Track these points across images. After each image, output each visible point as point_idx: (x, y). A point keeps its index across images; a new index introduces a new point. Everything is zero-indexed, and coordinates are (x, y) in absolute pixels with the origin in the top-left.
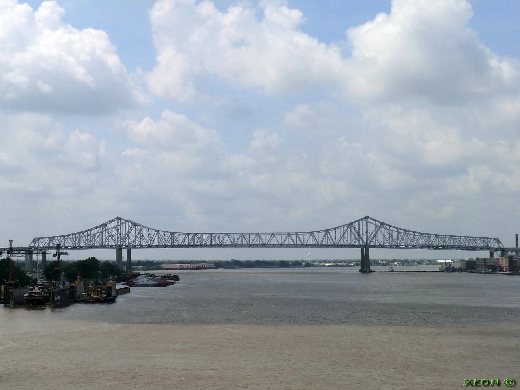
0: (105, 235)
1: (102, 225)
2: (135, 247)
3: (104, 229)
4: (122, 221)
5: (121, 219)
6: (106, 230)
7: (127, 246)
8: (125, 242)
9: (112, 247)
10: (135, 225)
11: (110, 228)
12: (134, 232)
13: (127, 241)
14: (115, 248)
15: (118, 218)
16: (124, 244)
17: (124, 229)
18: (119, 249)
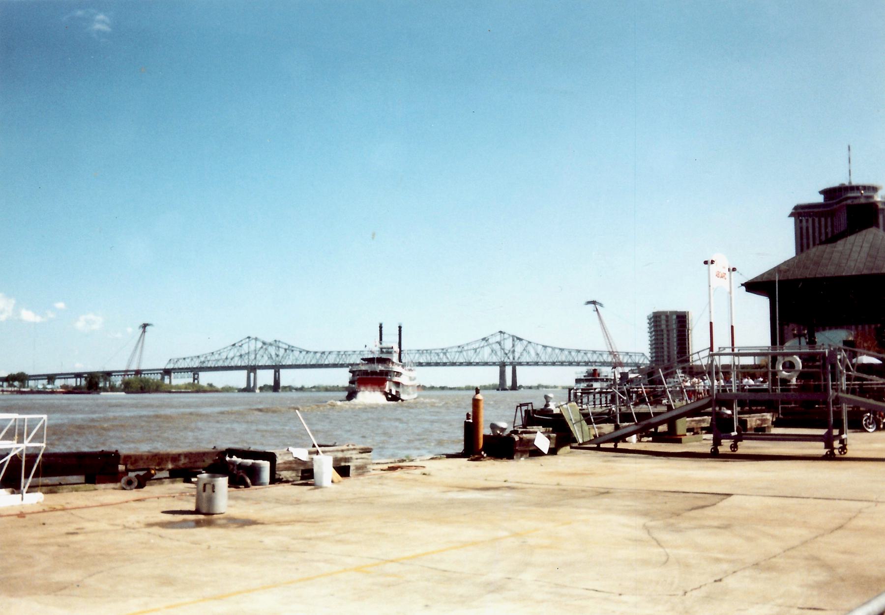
0: (487, 350)
1: (483, 339)
2: (520, 364)
3: (486, 344)
4: (506, 336)
5: (504, 333)
6: (488, 345)
7: (511, 364)
8: (509, 358)
9: (494, 364)
10: (520, 339)
11: (493, 344)
12: (519, 348)
13: (511, 358)
14: (498, 365)
15: (501, 332)
16: (508, 361)
17: (508, 344)
18: (503, 365)
